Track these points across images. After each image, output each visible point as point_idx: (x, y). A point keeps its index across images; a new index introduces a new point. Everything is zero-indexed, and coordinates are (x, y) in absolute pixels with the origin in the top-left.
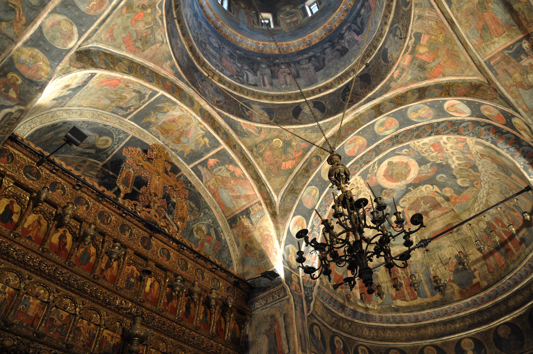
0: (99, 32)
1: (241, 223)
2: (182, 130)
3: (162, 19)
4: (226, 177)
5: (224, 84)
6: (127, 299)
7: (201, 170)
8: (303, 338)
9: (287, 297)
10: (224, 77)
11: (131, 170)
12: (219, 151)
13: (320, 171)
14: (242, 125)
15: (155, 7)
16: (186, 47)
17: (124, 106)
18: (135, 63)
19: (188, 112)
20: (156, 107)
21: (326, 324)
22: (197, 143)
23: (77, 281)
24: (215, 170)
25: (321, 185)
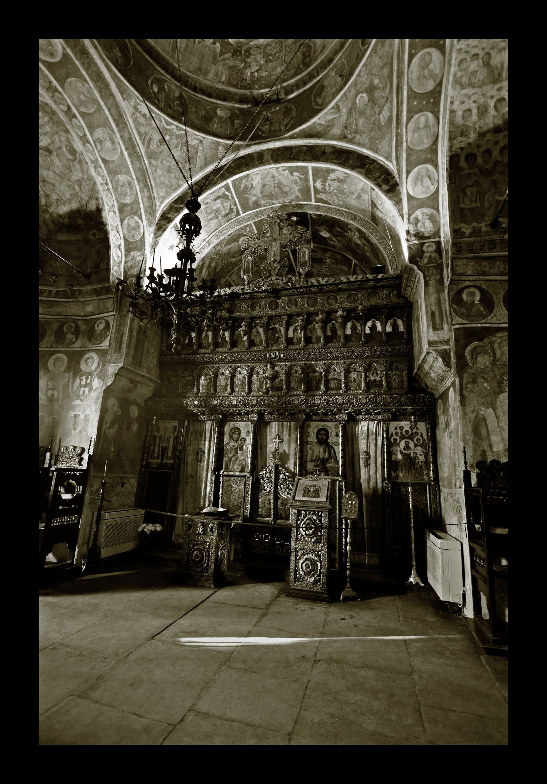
0: (156, 196)
1: (378, 216)
3: (181, 129)
5: (292, 92)
8: (437, 315)
9: (418, 277)
10: (288, 85)
12: (313, 173)
13: (410, 89)
14: (318, 122)
15: (167, 130)
16: (237, 105)
17: (227, 212)
18: (200, 180)
20: (243, 193)
21: (493, 278)
22: (296, 183)
24: (327, 189)
25: (428, 102)
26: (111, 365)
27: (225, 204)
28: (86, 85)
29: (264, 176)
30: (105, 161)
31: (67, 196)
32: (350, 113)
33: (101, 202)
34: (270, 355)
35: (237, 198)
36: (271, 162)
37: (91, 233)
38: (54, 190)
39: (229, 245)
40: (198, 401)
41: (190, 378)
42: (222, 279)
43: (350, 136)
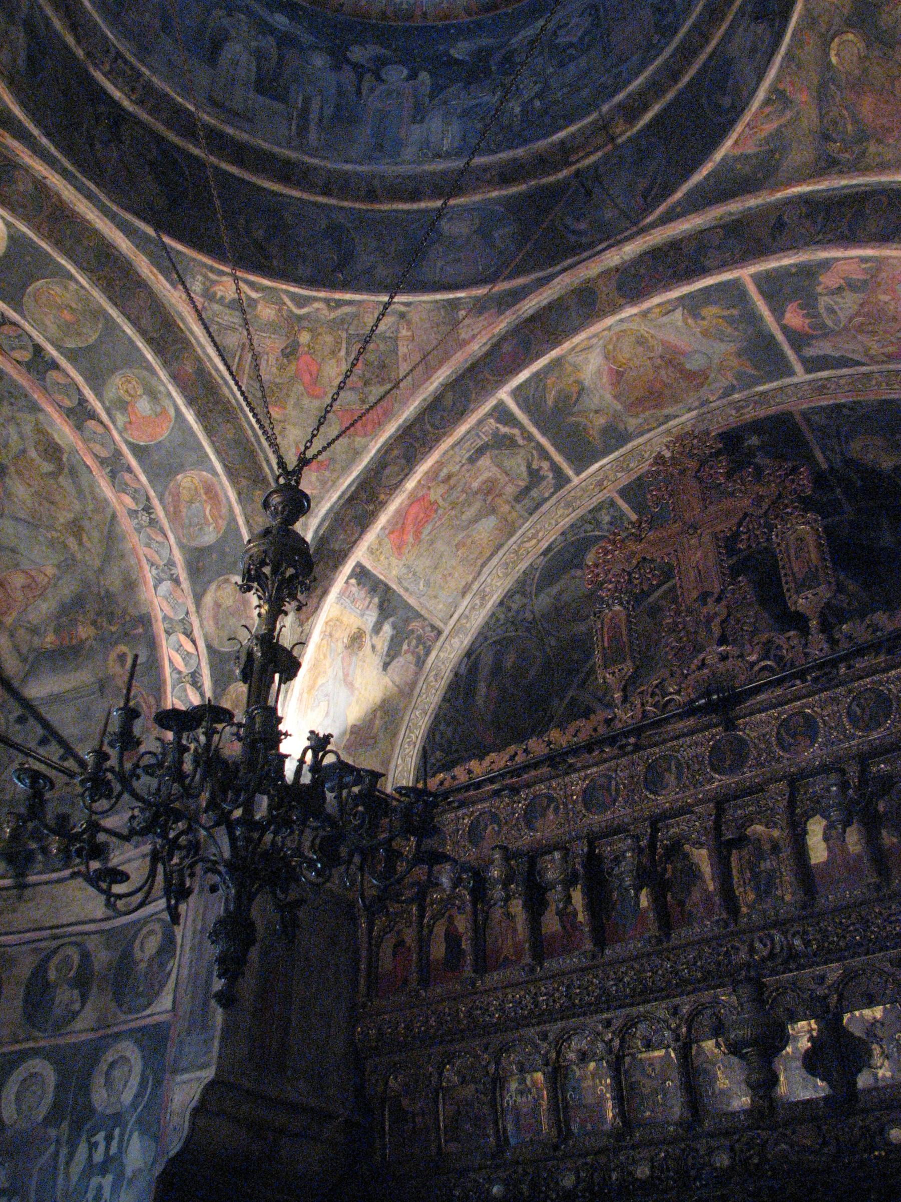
2: (659, 361)
3: (340, 303)
4: (862, 305)
5: (646, 108)
6: (764, 928)
7: (821, 353)
10: (630, 96)
11: (617, 608)
12: (762, 292)
14: (737, 152)
15: (300, 318)
16: (495, 194)
17: (522, 484)
19: (595, 336)
23: (621, 980)
24: (829, 323)
26: (179, 1078)
27: (508, 464)
28: (73, 286)
29: (610, 347)
30: (139, 451)
31: (50, 571)
32: (822, 96)
33: (133, 561)
34: (752, 950)
35: (544, 434)
36: (622, 301)
37: (113, 656)
38: (17, 565)
39: (550, 584)
40: (506, 1183)
41: (468, 1091)
42: (555, 702)
43: (847, 156)
